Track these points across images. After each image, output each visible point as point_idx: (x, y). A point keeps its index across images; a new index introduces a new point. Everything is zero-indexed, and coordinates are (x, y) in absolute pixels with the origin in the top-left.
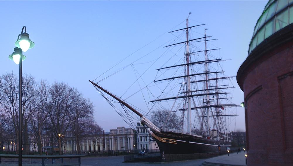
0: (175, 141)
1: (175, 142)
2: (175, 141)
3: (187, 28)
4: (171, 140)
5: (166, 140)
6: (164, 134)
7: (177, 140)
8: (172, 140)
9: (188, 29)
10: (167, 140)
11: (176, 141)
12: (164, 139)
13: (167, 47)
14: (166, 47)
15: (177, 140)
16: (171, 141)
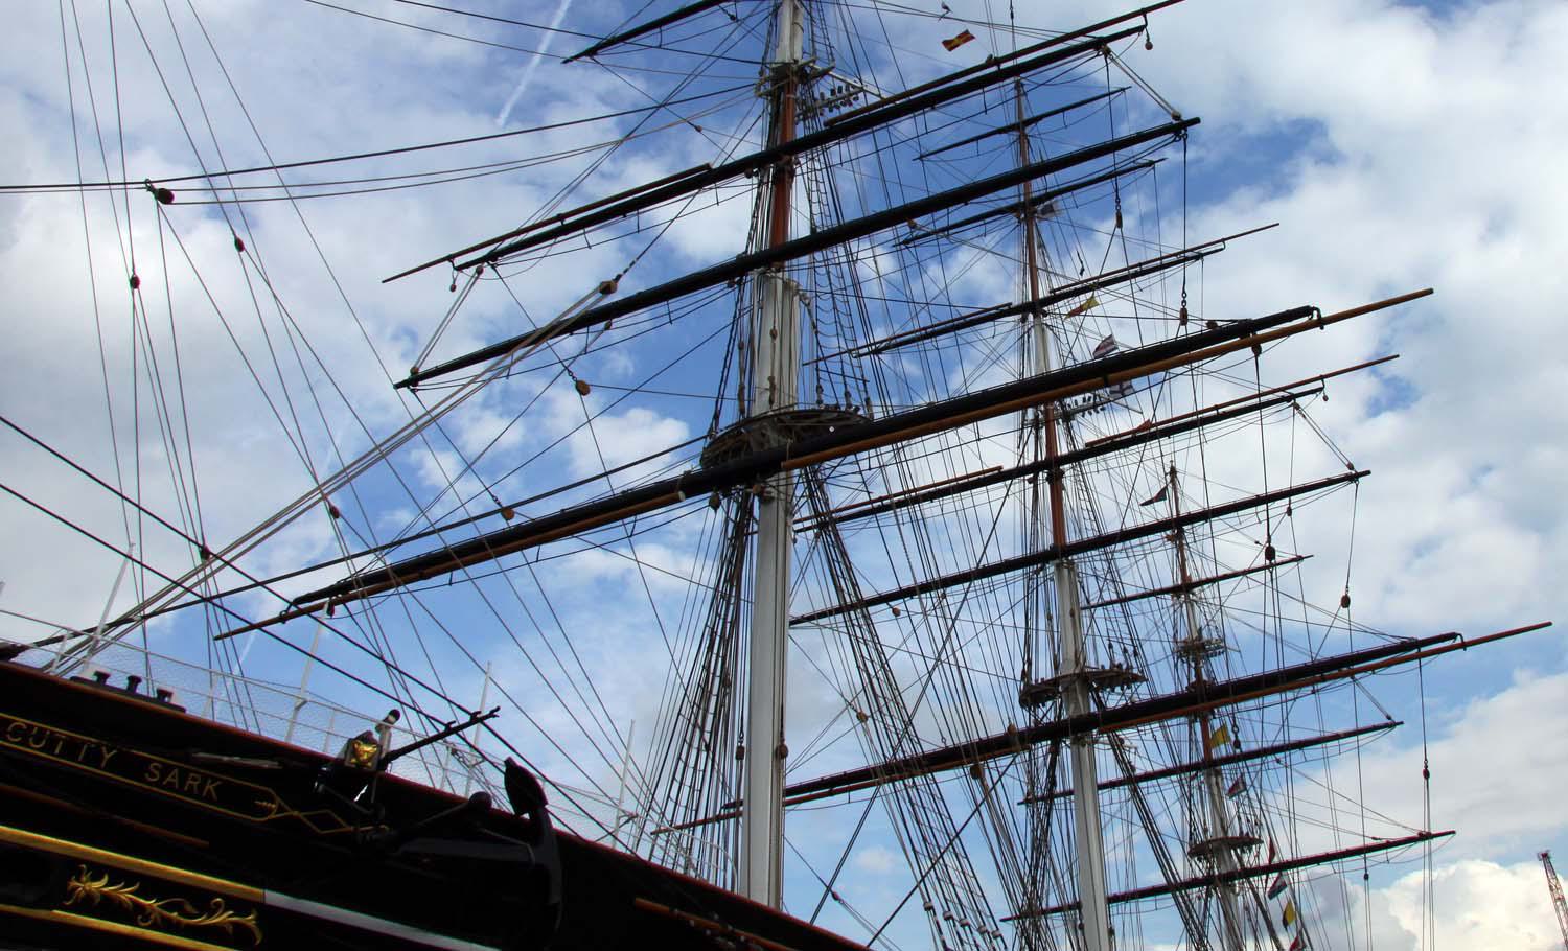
4: (119, 875)
7: (275, 898)
8: (151, 885)
11: (267, 913)
15: (275, 898)
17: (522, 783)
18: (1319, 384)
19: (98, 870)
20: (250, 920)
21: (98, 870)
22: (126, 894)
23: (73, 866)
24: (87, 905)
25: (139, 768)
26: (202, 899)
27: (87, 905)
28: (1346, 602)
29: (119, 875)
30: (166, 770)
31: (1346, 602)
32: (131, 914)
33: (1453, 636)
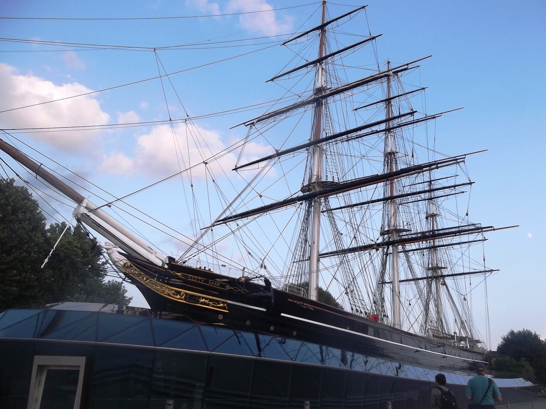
0: (223, 303)
1: (222, 305)
2: (223, 303)
3: (322, 28)
4: (206, 299)
5: (186, 294)
6: (179, 274)
7: (229, 302)
8: (211, 300)
9: (327, 28)
10: (189, 297)
12: (178, 293)
13: (275, 81)
14: (272, 80)
15: (229, 302)
16: (207, 301)
17: (267, 281)
18: (464, 156)
19: (203, 298)
20: (225, 305)
21: (203, 298)
22: (207, 301)
23: (199, 297)
24: (202, 303)
25: (208, 282)
26: (218, 302)
27: (202, 303)
28: (467, 214)
29: (206, 299)
30: (211, 282)
31: (467, 214)
32: (208, 305)
33: (492, 227)
